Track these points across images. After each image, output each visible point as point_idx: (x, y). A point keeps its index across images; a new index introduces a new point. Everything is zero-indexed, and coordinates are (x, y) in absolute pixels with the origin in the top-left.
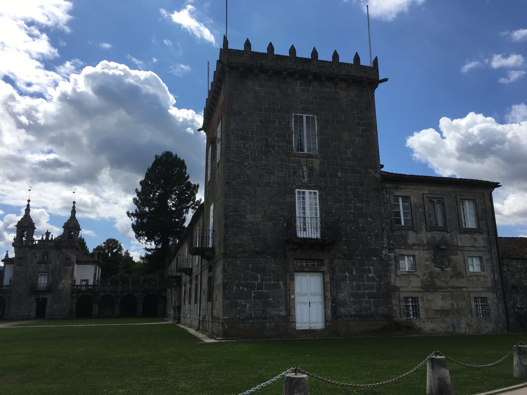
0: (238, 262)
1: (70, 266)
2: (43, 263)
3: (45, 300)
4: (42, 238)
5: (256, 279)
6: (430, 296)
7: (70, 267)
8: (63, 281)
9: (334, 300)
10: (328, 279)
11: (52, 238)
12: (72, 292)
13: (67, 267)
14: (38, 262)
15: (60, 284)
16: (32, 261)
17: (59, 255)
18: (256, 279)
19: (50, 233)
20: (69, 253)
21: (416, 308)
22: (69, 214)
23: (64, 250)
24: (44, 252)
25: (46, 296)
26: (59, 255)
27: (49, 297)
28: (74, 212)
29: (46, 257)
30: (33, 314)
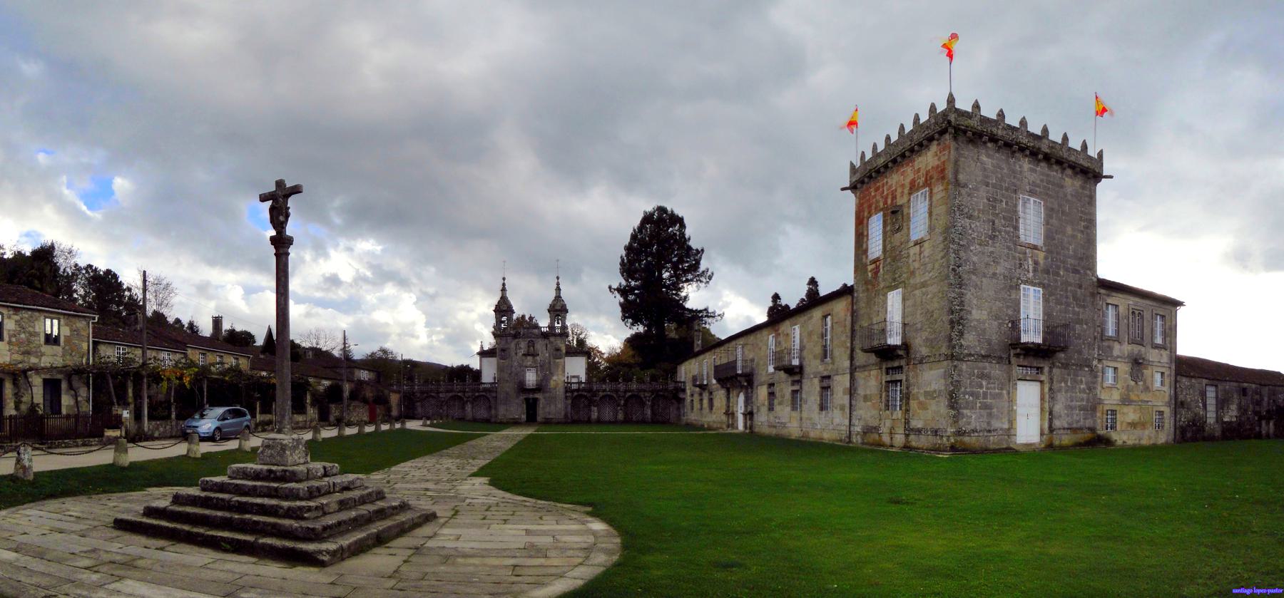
0: (964, 367)
5: (981, 386)
6: (1125, 409)
9: (1051, 413)
10: (1046, 390)
18: (981, 386)
21: (1114, 421)
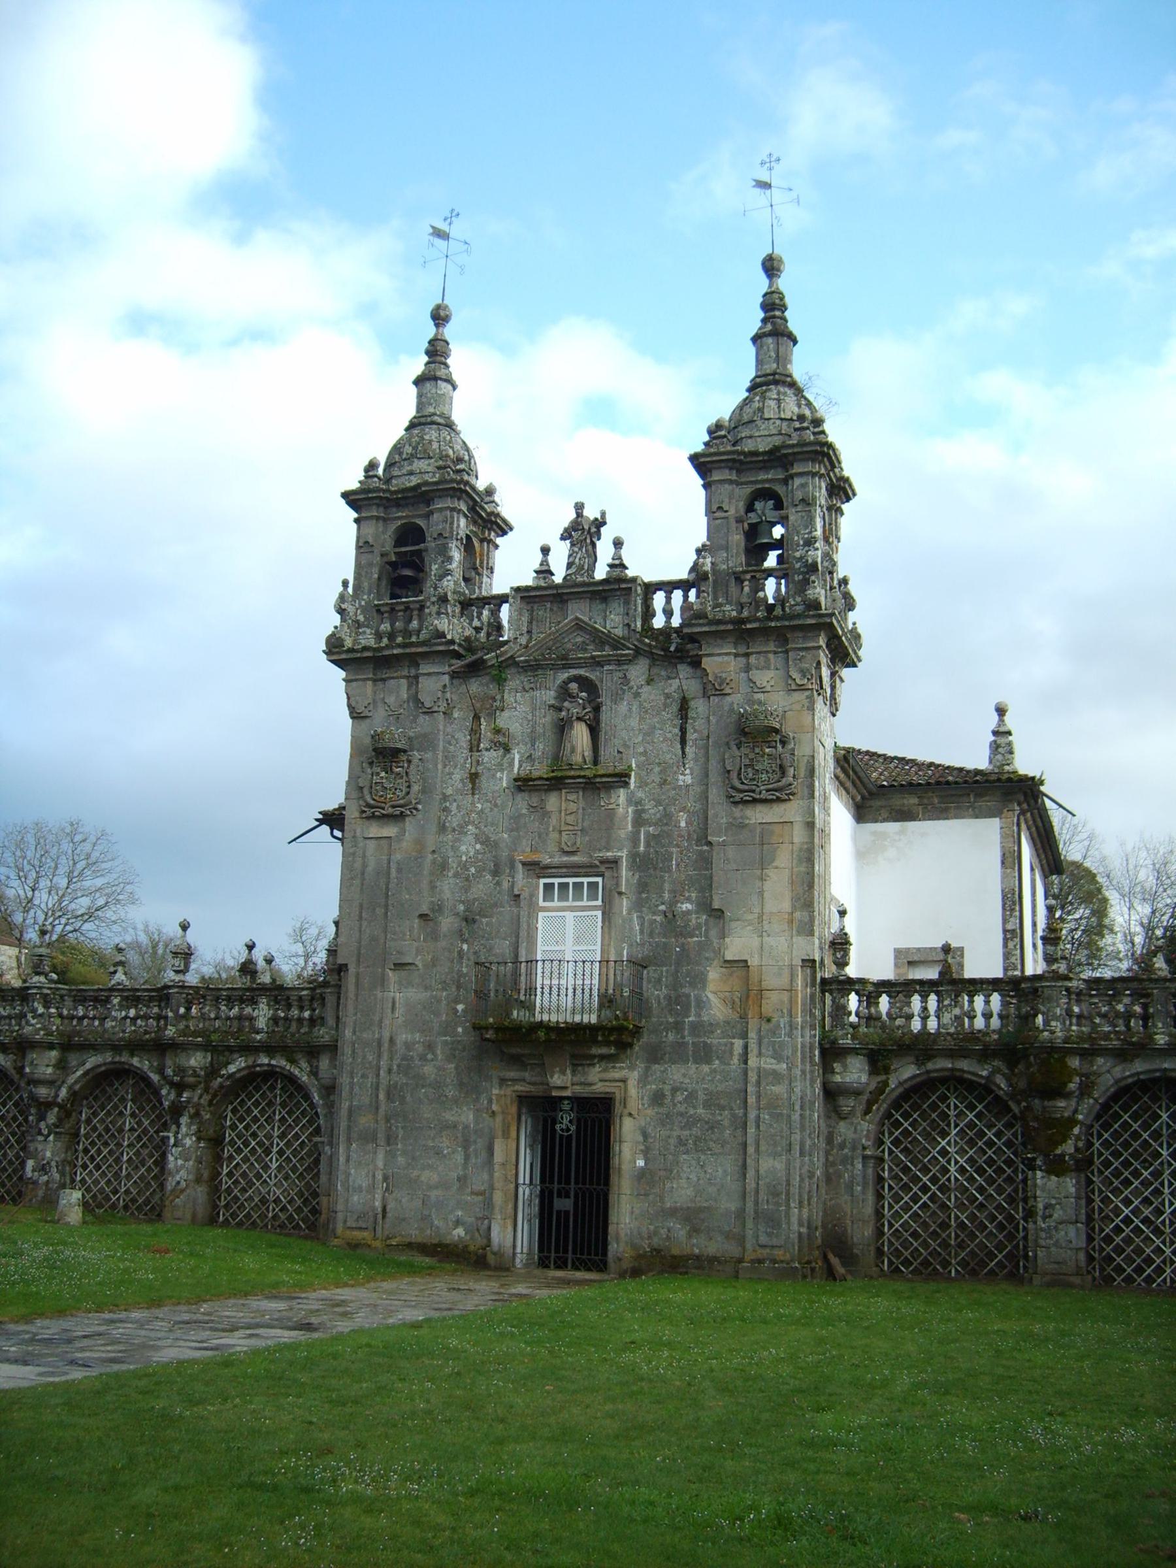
1: (779, 796)
2: (556, 783)
3: (598, 1114)
4: (544, 572)
7: (791, 811)
8: (739, 944)
11: (618, 565)
12: (831, 1053)
13: (758, 815)
14: (523, 784)
15: (714, 974)
16: (474, 777)
17: (684, 707)
19: (600, 523)
20: (766, 678)
22: (743, 367)
23: (721, 661)
24: (564, 693)
25: (598, 1079)
26: (684, 707)
27: (629, 1083)
28: (774, 330)
29: (580, 734)
30: (514, 1234)
